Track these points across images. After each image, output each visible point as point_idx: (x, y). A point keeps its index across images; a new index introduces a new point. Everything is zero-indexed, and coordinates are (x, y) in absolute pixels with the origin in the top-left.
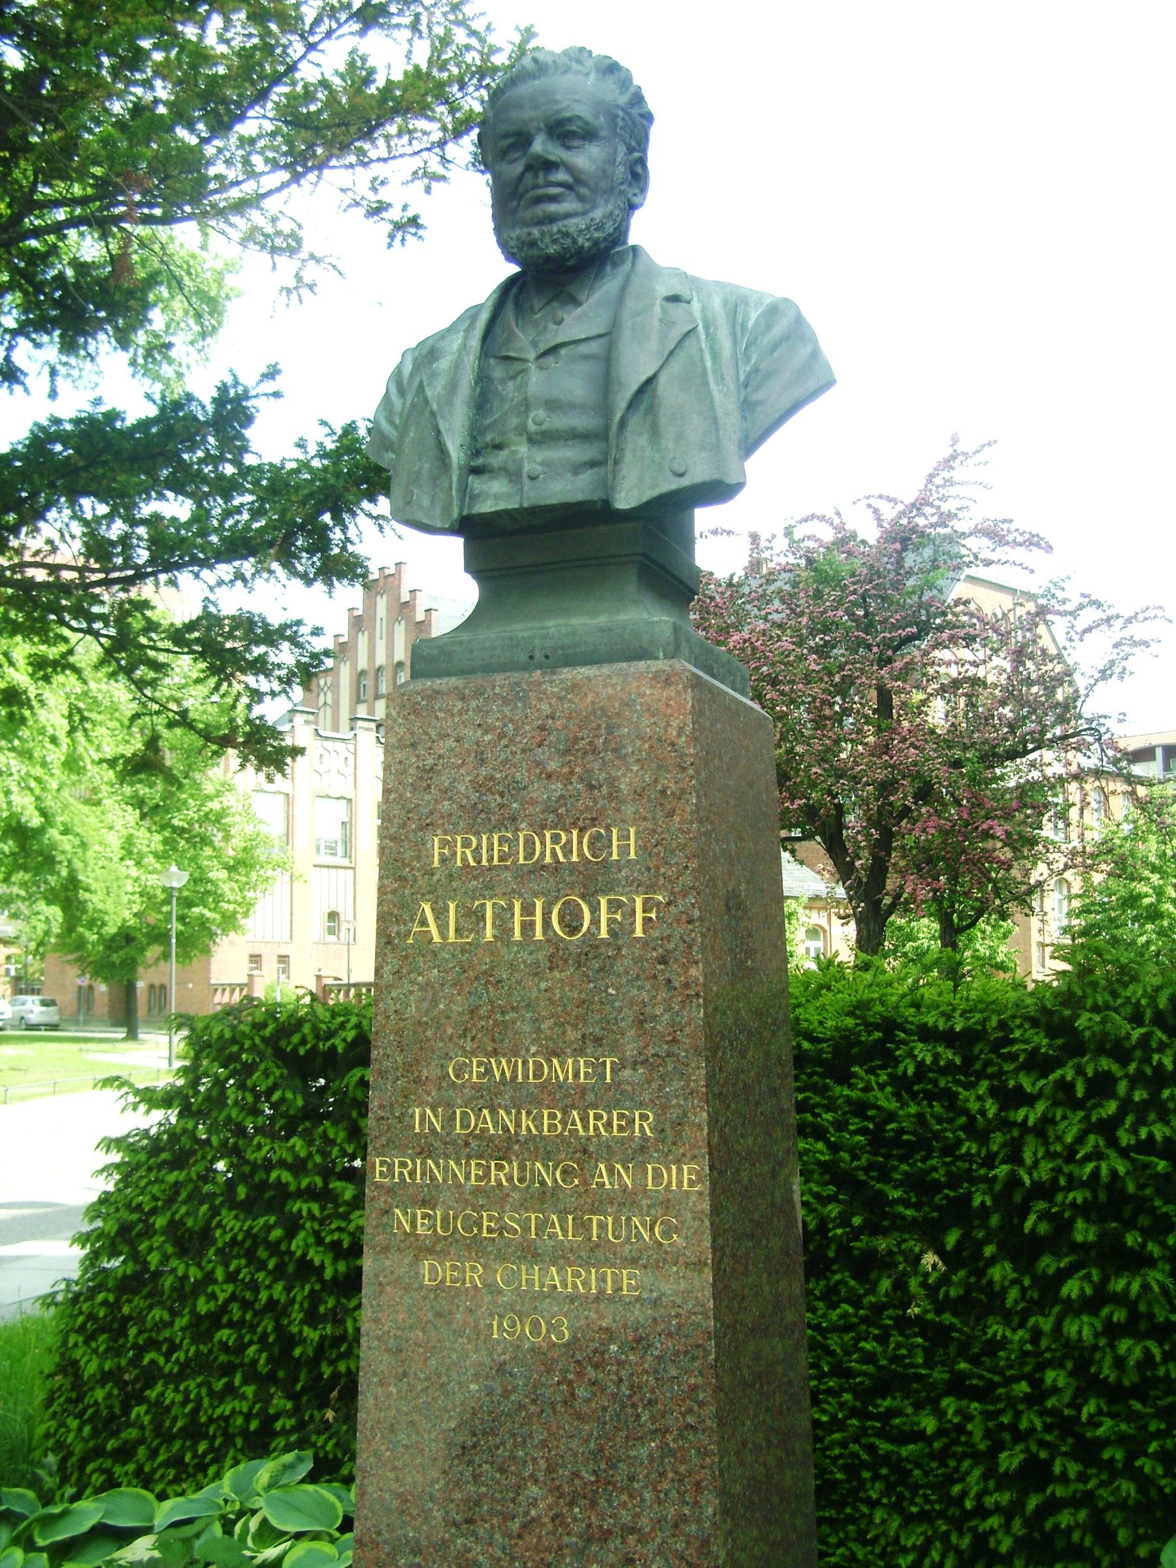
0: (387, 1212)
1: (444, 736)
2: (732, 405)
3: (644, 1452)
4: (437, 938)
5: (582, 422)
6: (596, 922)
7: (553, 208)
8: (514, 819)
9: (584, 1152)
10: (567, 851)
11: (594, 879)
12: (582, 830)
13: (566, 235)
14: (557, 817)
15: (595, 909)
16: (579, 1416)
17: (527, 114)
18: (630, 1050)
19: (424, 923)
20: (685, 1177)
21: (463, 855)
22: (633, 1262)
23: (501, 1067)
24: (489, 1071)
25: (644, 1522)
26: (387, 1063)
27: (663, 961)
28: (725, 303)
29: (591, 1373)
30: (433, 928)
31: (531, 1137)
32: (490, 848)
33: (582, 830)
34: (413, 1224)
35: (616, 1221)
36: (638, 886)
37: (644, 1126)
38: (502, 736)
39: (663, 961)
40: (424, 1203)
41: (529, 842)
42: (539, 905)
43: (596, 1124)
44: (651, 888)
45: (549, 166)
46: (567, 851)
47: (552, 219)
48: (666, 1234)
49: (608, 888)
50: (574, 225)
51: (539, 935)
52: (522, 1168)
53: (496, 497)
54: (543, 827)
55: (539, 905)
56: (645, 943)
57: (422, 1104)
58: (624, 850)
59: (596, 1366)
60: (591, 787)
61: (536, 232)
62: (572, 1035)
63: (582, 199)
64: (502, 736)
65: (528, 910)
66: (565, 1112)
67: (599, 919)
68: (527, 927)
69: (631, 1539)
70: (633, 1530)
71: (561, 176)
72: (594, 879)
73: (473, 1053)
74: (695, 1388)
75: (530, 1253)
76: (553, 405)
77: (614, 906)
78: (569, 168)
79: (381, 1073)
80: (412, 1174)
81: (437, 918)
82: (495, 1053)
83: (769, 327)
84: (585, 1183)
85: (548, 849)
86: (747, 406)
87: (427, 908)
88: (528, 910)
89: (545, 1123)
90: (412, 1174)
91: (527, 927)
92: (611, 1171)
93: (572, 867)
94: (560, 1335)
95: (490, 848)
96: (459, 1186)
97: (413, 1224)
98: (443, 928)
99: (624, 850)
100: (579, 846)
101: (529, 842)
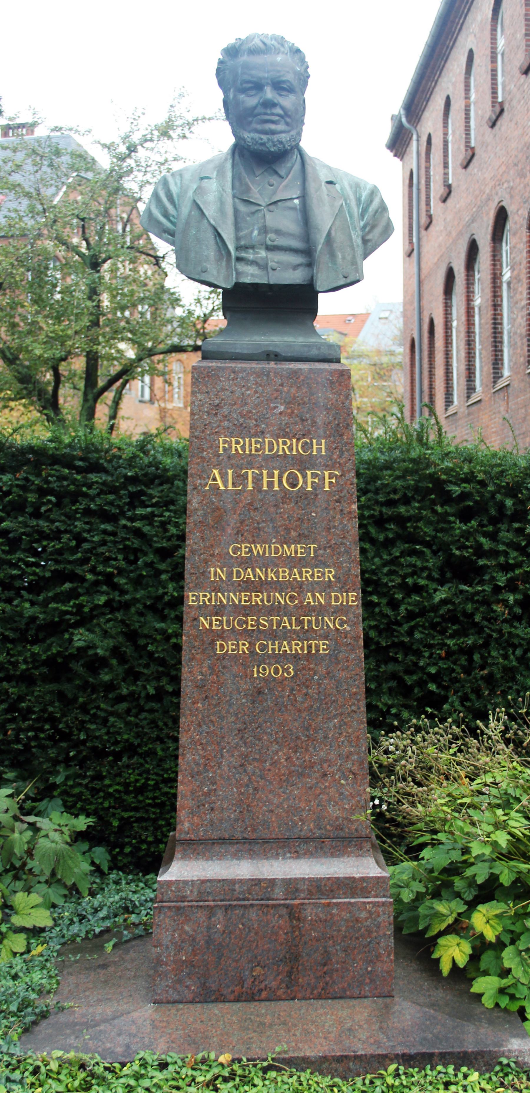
0: (196, 619)
1: (223, 390)
2: (359, 241)
3: (331, 725)
4: (222, 488)
5: (295, 244)
6: (305, 482)
7: (273, 127)
8: (263, 433)
9: (300, 587)
10: (290, 449)
11: (303, 463)
12: (298, 440)
13: (281, 143)
14: (284, 433)
15: (305, 477)
16: (299, 711)
17: (261, 74)
18: (323, 542)
19: (215, 479)
20: (353, 598)
21: (236, 448)
22: (326, 638)
23: (258, 549)
24: (251, 551)
25: (332, 757)
26: (195, 547)
27: (338, 501)
28: (351, 187)
29: (305, 690)
30: (219, 482)
31: (273, 582)
32: (250, 445)
33: (298, 440)
34: (211, 625)
35: (317, 620)
36: (327, 467)
37: (330, 574)
38: (256, 392)
39: (338, 501)
40: (217, 614)
41: (271, 444)
42: (276, 473)
43: (307, 574)
44: (332, 467)
45: (274, 105)
46: (290, 449)
47: (273, 133)
48: (341, 625)
49: (313, 467)
50: (284, 137)
51: (276, 488)
52: (269, 597)
53: (252, 275)
54: (278, 437)
55: (276, 473)
56: (329, 493)
57: (215, 567)
58: (319, 450)
59: (307, 687)
60: (303, 420)
61: (265, 138)
62: (293, 534)
63: (287, 124)
64: (256, 392)
65: (271, 475)
66: (291, 570)
67: (307, 481)
68: (270, 484)
69: (325, 765)
70: (326, 761)
71: (278, 111)
72: (303, 463)
73: (242, 542)
74: (355, 694)
75: (273, 635)
76: (278, 232)
77: (314, 476)
78: (282, 108)
79: (193, 552)
80: (210, 600)
81: (222, 477)
82: (254, 542)
83: (371, 201)
84: (301, 602)
85: (281, 447)
86: (365, 241)
87: (216, 472)
88: (271, 475)
89: (284, 574)
90: (210, 600)
91: (270, 484)
92: (314, 596)
93: (293, 457)
94: (289, 673)
95: (250, 445)
96: (234, 604)
97: (211, 625)
98: (225, 483)
99: (319, 450)
100: (297, 447)
101: (271, 444)
